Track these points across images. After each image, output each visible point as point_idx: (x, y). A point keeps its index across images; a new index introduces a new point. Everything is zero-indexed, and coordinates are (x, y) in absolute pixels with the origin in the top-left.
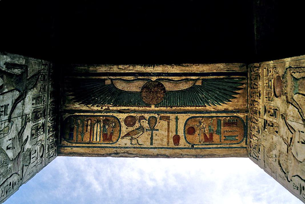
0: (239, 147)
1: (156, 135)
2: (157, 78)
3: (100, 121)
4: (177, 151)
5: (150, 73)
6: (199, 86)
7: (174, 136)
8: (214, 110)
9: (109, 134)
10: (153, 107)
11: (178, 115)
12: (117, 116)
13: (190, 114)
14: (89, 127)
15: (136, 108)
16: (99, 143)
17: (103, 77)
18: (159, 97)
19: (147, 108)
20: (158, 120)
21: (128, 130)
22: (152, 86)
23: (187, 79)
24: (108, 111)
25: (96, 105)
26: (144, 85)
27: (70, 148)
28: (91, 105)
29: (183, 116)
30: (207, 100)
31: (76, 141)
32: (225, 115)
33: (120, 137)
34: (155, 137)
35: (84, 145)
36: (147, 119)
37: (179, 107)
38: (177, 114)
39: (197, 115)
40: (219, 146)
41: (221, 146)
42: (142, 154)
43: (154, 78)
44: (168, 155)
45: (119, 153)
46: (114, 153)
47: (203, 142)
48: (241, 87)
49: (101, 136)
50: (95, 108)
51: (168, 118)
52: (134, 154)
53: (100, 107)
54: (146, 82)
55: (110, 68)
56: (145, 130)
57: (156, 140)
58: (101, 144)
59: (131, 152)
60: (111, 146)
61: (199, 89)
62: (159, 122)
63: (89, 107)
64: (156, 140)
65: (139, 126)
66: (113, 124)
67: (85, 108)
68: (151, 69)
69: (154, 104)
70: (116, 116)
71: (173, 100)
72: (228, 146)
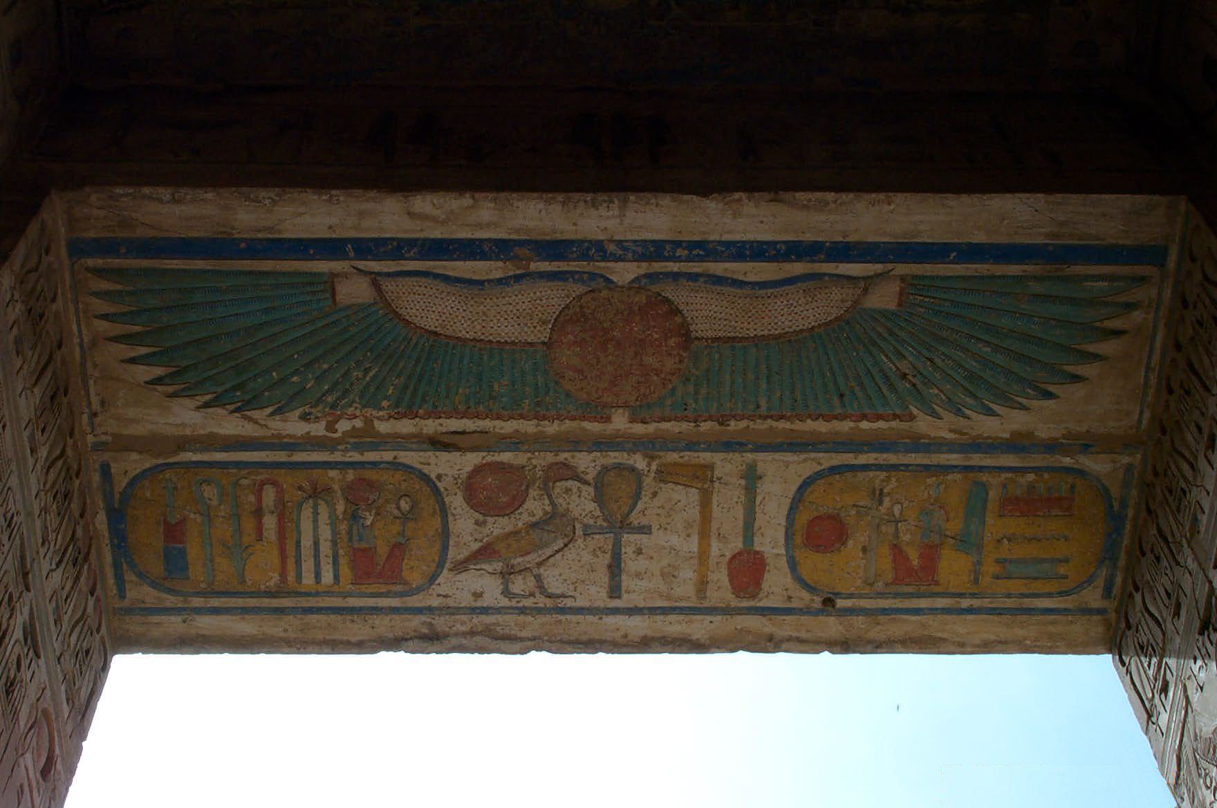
0: (1065, 610)
1: (639, 552)
2: (642, 272)
3: (328, 490)
4: (753, 623)
5: (599, 246)
6: (884, 313)
7: (734, 557)
8: (956, 436)
9: (383, 551)
10: (620, 422)
11: (760, 456)
12: (421, 463)
13: (821, 455)
14: (270, 522)
15: (529, 427)
16: (329, 593)
17: (323, 266)
18: (656, 370)
19: (587, 425)
20: (648, 481)
21: (486, 531)
22: (615, 315)
23: (819, 276)
24: (366, 438)
25: (297, 413)
26: (567, 306)
27: (179, 619)
28: (270, 410)
29: (787, 464)
30: (919, 386)
31: (203, 585)
32: (1009, 460)
33: (448, 565)
34: (631, 564)
35: (252, 602)
36: (589, 478)
37: (766, 418)
38: (752, 451)
39: (862, 459)
40: (965, 603)
41: (976, 603)
42: (565, 637)
43: (625, 272)
44: (703, 641)
45: (446, 636)
46: (416, 637)
47: (887, 585)
48: (1116, 324)
49: (343, 561)
50: (294, 426)
51: (702, 477)
52: (521, 639)
53: (324, 423)
54: (579, 289)
55: (362, 214)
56: (579, 532)
57: (638, 575)
58: (345, 595)
59: (507, 631)
60: (399, 605)
61: (880, 330)
62: (655, 494)
63: (256, 422)
64: (638, 575)
65: (546, 513)
66: (404, 505)
67: (230, 425)
68: (608, 218)
69: (625, 406)
70: (419, 466)
71: (733, 383)
72: (1010, 603)
